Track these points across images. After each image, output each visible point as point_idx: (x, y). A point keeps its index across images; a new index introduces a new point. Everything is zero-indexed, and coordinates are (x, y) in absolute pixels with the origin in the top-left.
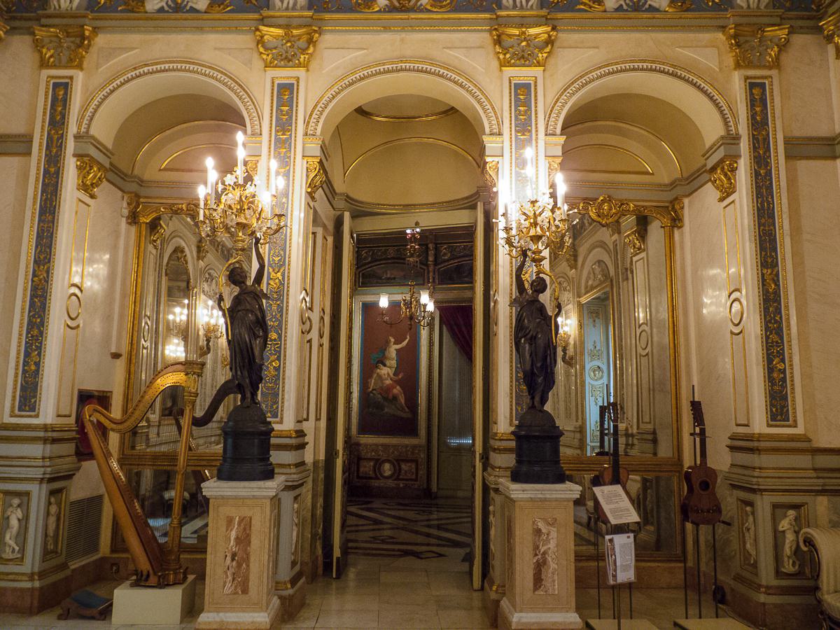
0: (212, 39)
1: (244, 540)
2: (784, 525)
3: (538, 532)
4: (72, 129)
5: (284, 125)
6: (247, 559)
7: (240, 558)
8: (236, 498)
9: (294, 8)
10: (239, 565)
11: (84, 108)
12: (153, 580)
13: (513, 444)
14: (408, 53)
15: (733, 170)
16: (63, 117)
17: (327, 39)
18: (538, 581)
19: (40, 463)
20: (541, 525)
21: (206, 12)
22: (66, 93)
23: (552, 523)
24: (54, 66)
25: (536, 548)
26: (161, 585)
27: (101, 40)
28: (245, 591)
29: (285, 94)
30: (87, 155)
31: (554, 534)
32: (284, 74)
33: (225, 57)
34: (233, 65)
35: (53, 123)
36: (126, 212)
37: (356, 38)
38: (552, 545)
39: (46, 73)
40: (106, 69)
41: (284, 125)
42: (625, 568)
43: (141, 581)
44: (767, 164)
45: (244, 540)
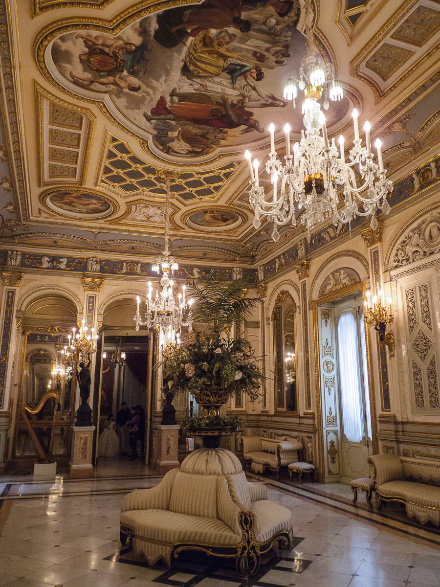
0: (66, 279)
1: (85, 443)
2: (238, 436)
3: (168, 439)
4: (15, 308)
5: (91, 310)
6: (86, 449)
7: (84, 449)
8: (83, 431)
9: (96, 272)
10: (84, 451)
11: (19, 300)
12: (47, 461)
13: (162, 415)
14: (132, 288)
15: (230, 330)
16: (12, 304)
17: (106, 282)
18: (168, 452)
19: (4, 424)
20: (169, 437)
21: (64, 270)
22: (13, 295)
23: (173, 436)
24: (9, 285)
25: (168, 443)
26: (49, 462)
27: (26, 276)
28: (85, 458)
29: (92, 300)
30: (20, 318)
31: (173, 439)
32: (91, 293)
33: (70, 285)
34: (74, 289)
35: (8, 305)
36: (21, 331)
37: (115, 282)
38: (172, 442)
39: (5, 287)
40: (27, 287)
41: (91, 310)
42: (191, 447)
43: (41, 461)
44: (239, 329)
45: (85, 443)
